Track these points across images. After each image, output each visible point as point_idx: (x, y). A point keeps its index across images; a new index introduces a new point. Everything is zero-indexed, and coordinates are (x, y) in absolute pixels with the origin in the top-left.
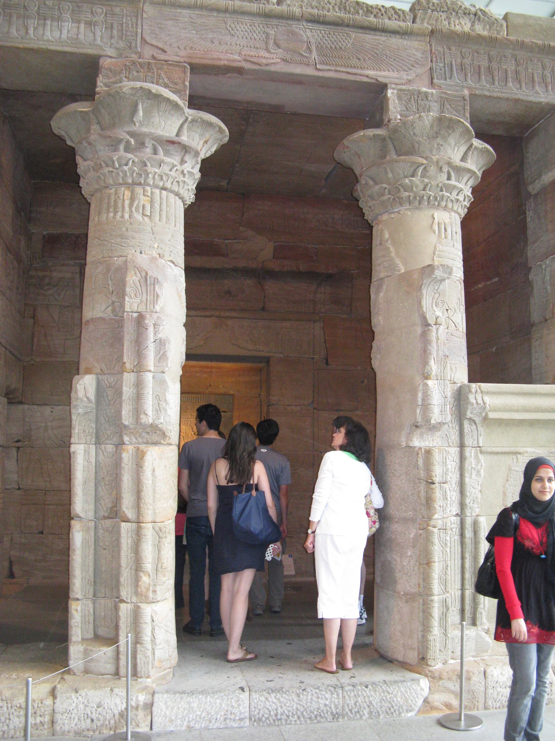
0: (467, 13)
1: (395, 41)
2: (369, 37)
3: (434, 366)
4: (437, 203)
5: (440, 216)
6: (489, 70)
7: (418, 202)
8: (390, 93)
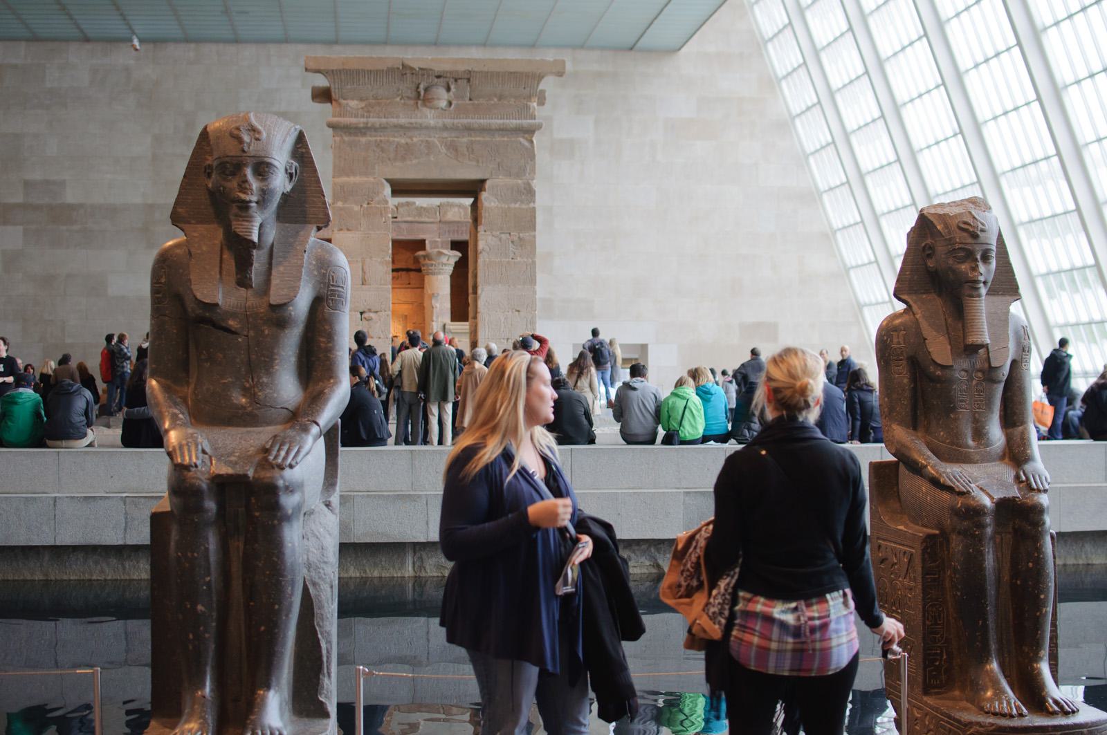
0: (457, 206)
1: (429, 225)
2: (421, 225)
3: (434, 318)
4: (439, 273)
5: (440, 277)
6: (457, 231)
7: (434, 274)
8: (427, 242)
